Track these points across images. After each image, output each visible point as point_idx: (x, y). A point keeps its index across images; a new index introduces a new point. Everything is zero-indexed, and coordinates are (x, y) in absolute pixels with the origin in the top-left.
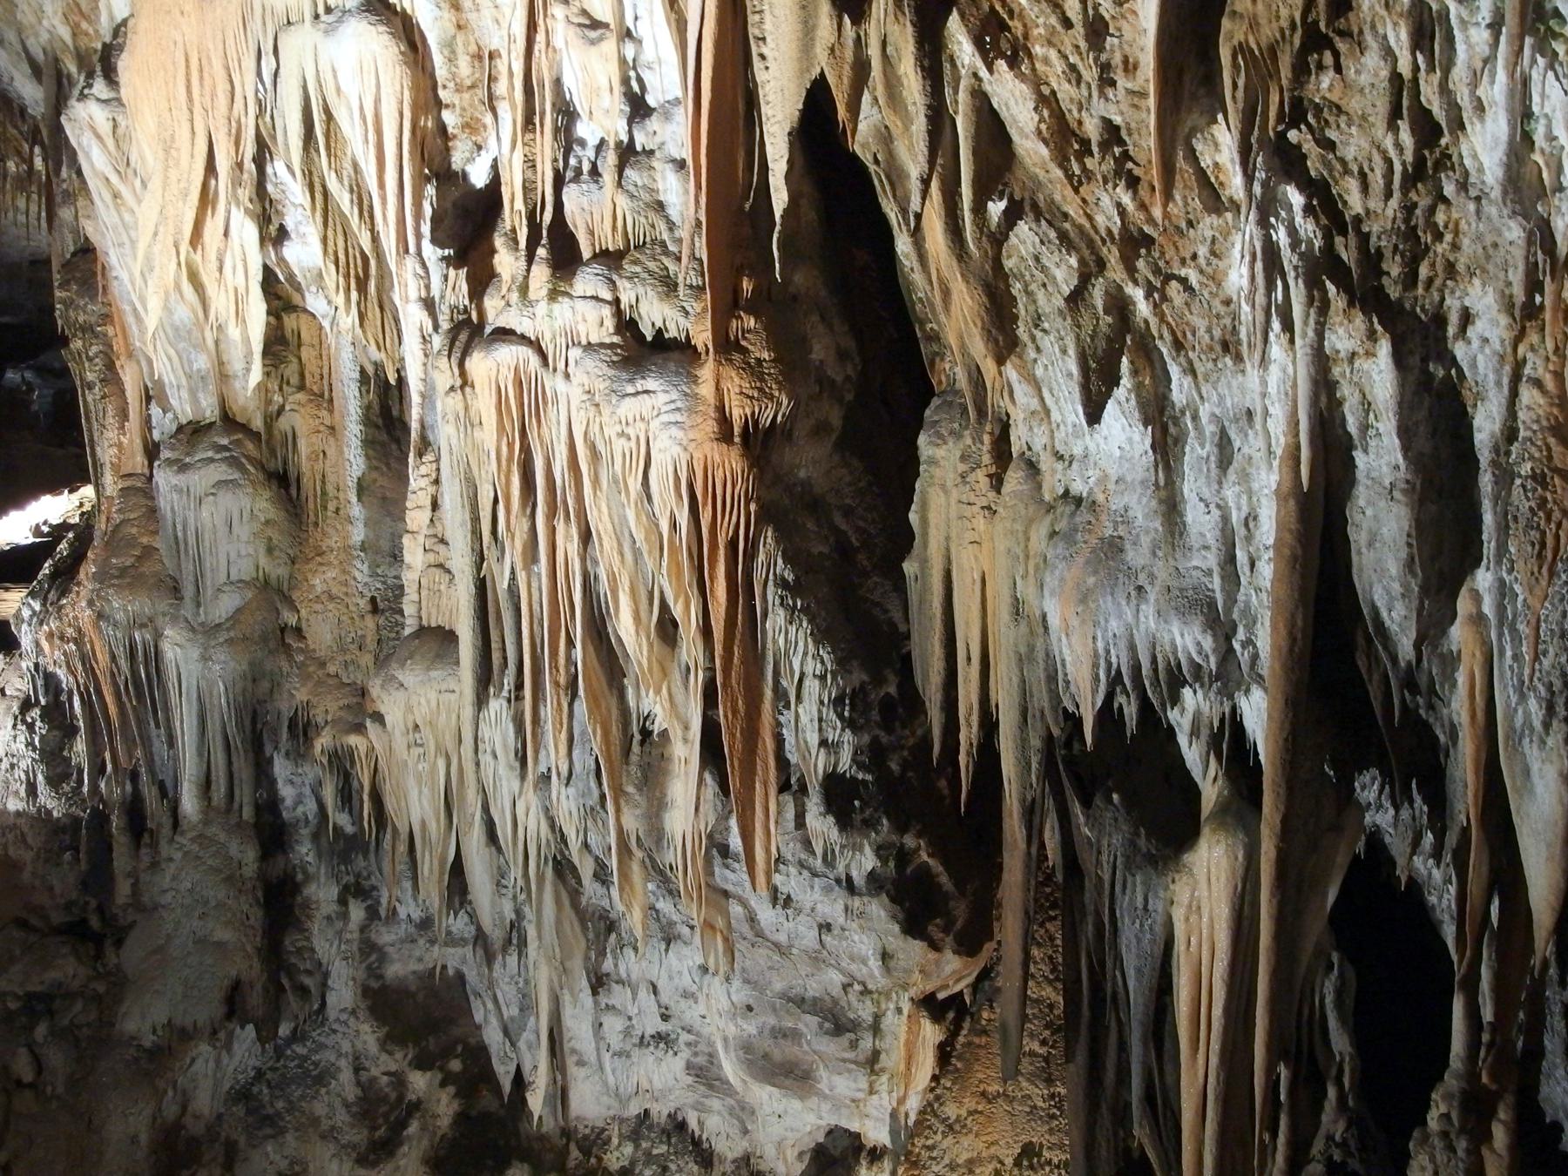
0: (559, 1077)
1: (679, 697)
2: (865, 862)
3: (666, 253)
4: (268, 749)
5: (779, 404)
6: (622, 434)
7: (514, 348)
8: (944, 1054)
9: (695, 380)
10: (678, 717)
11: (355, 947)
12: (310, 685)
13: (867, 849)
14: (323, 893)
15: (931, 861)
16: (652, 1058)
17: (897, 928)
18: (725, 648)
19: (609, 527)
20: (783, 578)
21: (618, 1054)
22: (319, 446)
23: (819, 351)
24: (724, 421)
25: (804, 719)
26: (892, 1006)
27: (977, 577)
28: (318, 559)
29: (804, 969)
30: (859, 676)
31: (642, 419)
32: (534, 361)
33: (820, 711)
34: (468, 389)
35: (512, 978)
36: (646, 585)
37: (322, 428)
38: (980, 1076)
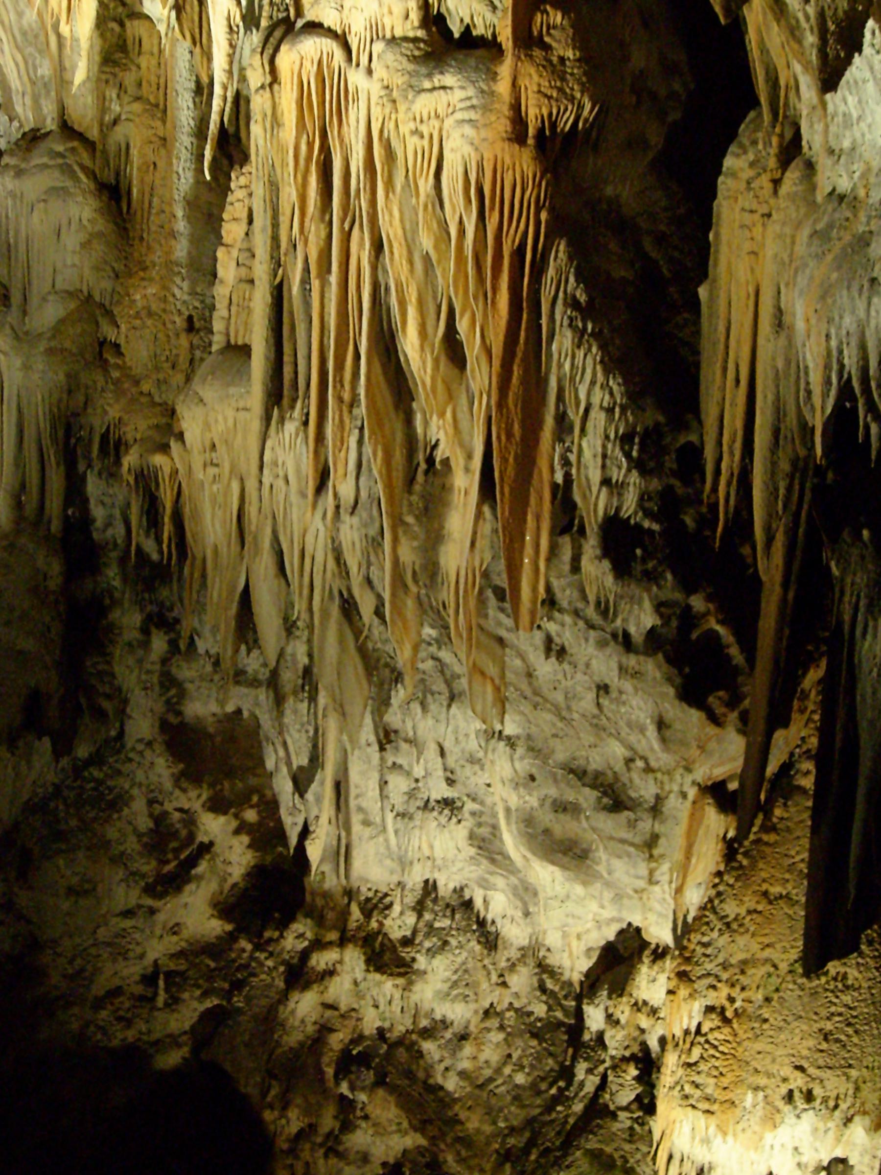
0: (343, 834)
1: (464, 424)
2: (642, 619)
4: (81, 467)
5: (581, 107)
6: (416, 132)
7: (318, 40)
8: (730, 850)
9: (493, 76)
10: (462, 445)
11: (155, 679)
12: (123, 401)
13: (647, 604)
14: (129, 619)
15: (718, 628)
16: (435, 823)
17: (671, 691)
18: (503, 366)
19: (400, 232)
20: (574, 297)
21: (402, 815)
22: (151, 158)
23: (638, 59)
24: (518, 121)
25: (587, 454)
26: (676, 788)
27: (751, 290)
28: (141, 274)
29: (588, 738)
30: (652, 416)
31: (437, 116)
32: (339, 55)
33: (604, 447)
34: (276, 87)
35: (303, 725)
36: (435, 297)
37: (154, 139)
38: (764, 875)
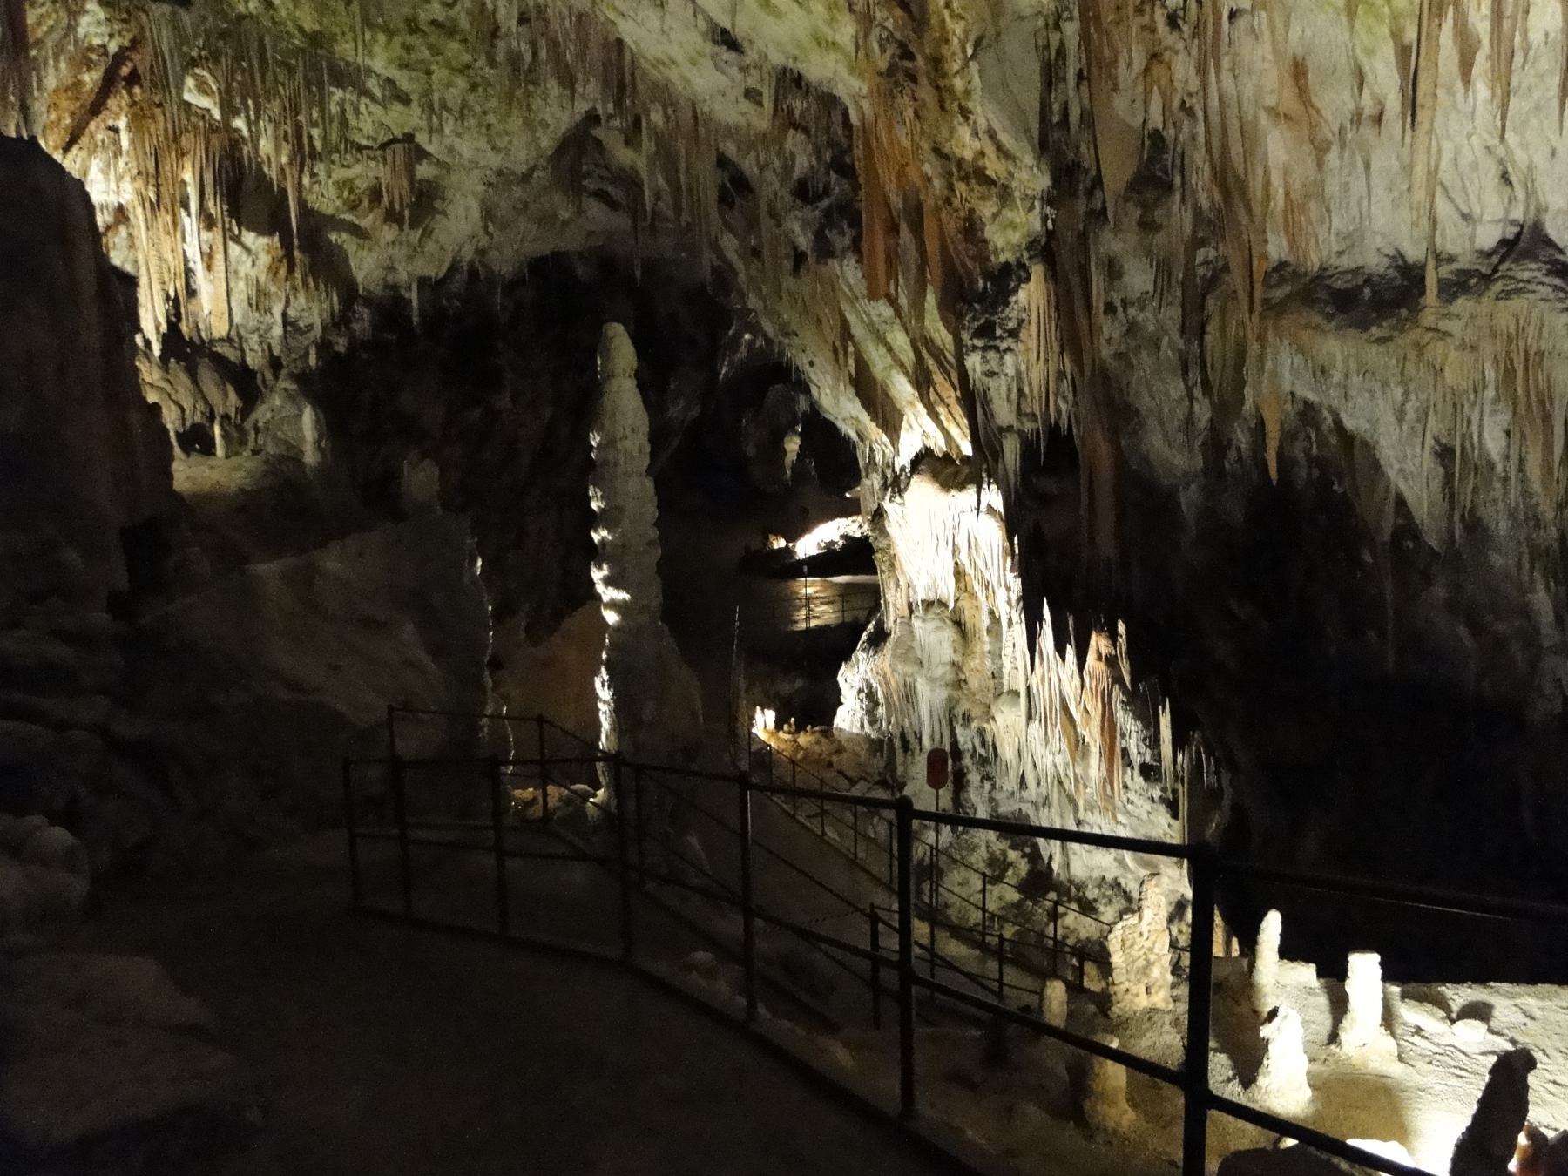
14: (974, 777)
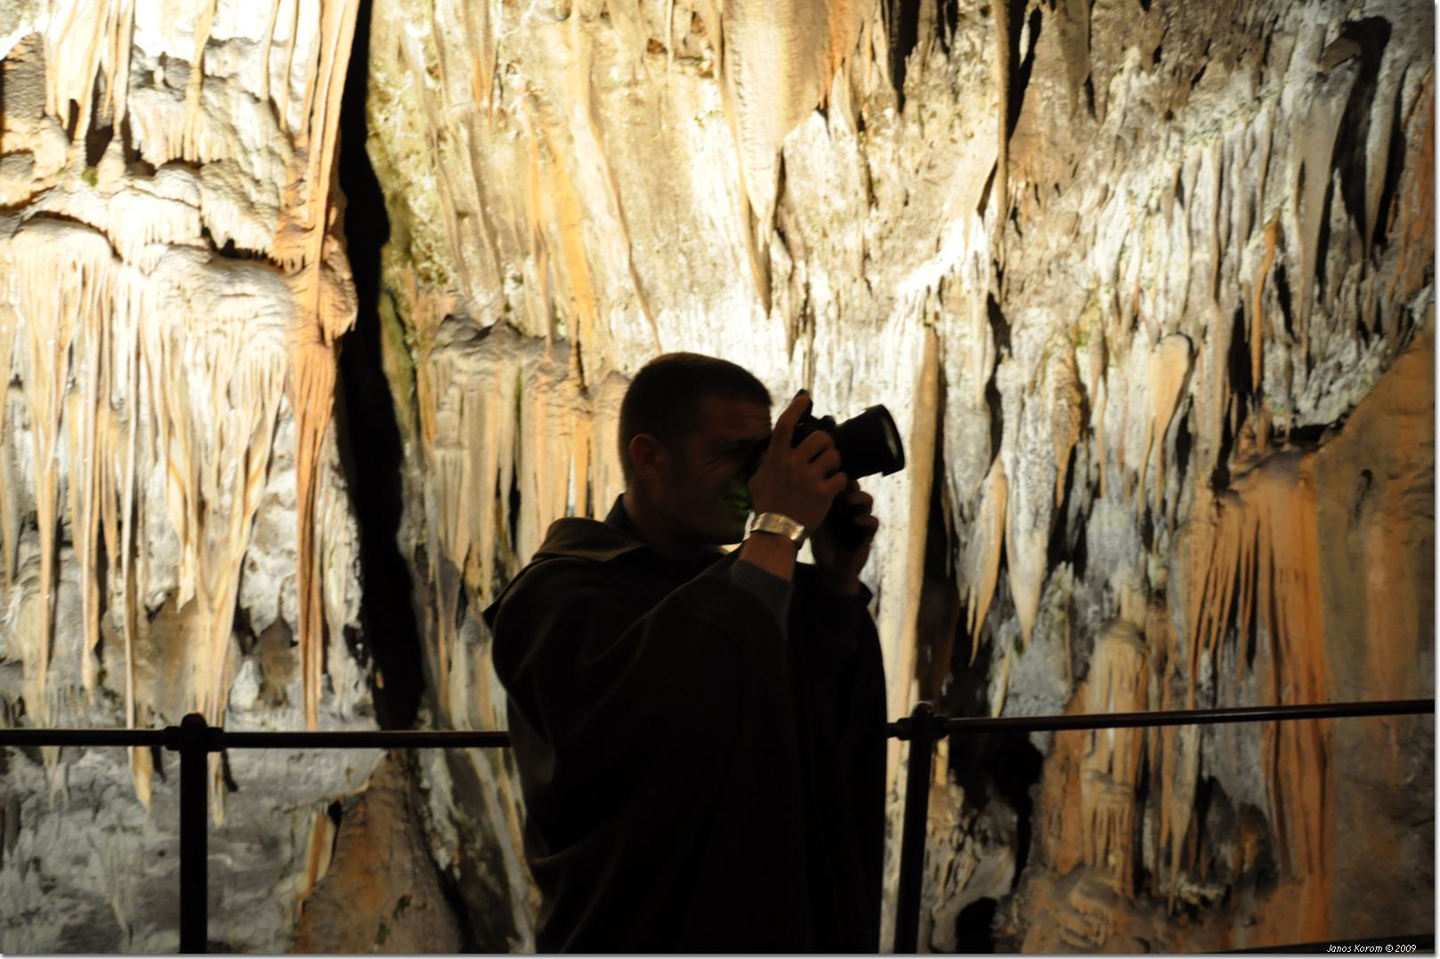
3: (245, 174)
